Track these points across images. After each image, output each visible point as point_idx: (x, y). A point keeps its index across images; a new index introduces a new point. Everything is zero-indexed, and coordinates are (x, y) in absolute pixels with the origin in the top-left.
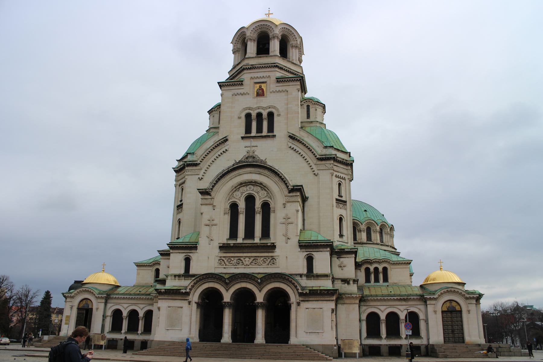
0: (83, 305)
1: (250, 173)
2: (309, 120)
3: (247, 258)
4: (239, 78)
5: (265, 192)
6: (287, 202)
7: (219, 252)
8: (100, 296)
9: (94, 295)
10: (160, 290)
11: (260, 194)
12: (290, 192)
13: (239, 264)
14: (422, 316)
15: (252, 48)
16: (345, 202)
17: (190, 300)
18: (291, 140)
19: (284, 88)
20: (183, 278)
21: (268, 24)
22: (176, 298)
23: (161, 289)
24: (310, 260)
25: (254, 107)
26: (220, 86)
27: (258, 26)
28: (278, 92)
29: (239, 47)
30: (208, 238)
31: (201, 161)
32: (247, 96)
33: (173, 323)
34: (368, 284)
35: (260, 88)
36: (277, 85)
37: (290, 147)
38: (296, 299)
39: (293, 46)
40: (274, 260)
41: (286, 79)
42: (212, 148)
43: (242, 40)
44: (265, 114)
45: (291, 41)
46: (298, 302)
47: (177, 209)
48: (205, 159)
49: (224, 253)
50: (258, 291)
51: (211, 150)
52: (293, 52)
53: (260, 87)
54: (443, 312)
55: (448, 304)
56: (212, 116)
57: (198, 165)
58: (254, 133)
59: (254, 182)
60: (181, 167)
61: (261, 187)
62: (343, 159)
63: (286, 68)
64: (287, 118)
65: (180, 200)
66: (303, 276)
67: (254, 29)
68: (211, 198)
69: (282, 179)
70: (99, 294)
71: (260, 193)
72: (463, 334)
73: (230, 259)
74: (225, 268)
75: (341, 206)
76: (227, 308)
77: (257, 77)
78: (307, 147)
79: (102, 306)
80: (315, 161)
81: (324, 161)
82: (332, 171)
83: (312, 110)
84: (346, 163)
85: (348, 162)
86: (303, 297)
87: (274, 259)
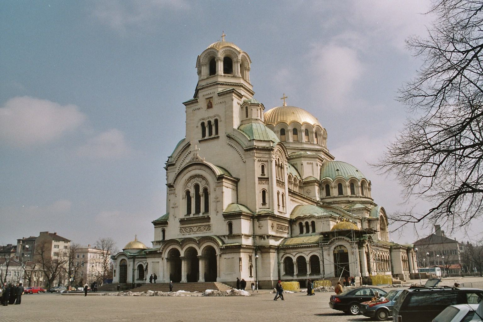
1: (195, 169)
3: (195, 227)
5: (205, 181)
11: (202, 183)
14: (320, 259)
15: (205, 70)
16: (268, 178)
17: (163, 257)
19: (223, 100)
24: (230, 225)
27: (207, 53)
31: (176, 162)
34: (301, 235)
37: (228, 144)
40: (210, 227)
44: (213, 122)
49: (183, 224)
50: (198, 249)
51: (181, 153)
52: (235, 67)
53: (210, 101)
54: (335, 254)
55: (339, 248)
58: (207, 137)
61: (202, 178)
62: (264, 147)
63: (226, 83)
67: (204, 56)
74: (183, 235)
75: (264, 182)
79: (132, 263)
82: (255, 158)
84: (268, 149)
85: (269, 148)
87: (210, 226)
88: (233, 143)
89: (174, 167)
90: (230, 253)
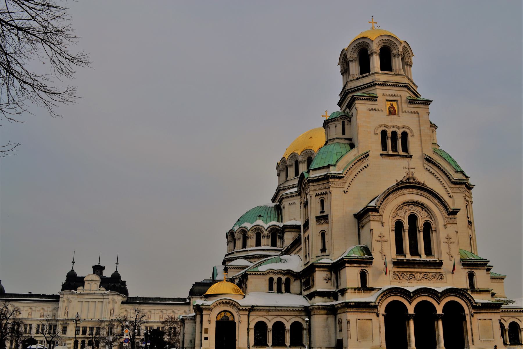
0: (221, 317)
3: (418, 273)
4: (367, 92)
5: (426, 213)
6: (447, 223)
7: (392, 267)
9: (237, 307)
10: (350, 304)
12: (448, 215)
13: (411, 278)
15: (375, 62)
17: (378, 313)
18: (427, 162)
19: (416, 110)
20: (363, 291)
22: (364, 311)
23: (351, 303)
24: (471, 276)
25: (389, 125)
28: (409, 113)
29: (355, 56)
30: (381, 253)
31: (345, 175)
32: (381, 112)
35: (392, 106)
36: (408, 106)
37: (426, 169)
38: (470, 311)
39: (408, 64)
40: (441, 275)
43: (360, 50)
45: (405, 58)
46: (473, 314)
47: (316, 220)
48: (348, 173)
49: (397, 268)
50: (438, 305)
51: (354, 164)
52: (407, 70)
53: (392, 105)
56: (334, 126)
57: (342, 178)
59: (415, 203)
60: (320, 177)
64: (421, 139)
65: (320, 211)
66: (469, 291)
68: (379, 215)
71: (421, 213)
73: (404, 274)
74: (399, 282)
76: (411, 320)
78: (443, 170)
79: (244, 319)
80: (450, 184)
81: (457, 185)
85: (470, 186)
86: (475, 309)
87: (442, 274)
88: (434, 169)
90: (486, 312)
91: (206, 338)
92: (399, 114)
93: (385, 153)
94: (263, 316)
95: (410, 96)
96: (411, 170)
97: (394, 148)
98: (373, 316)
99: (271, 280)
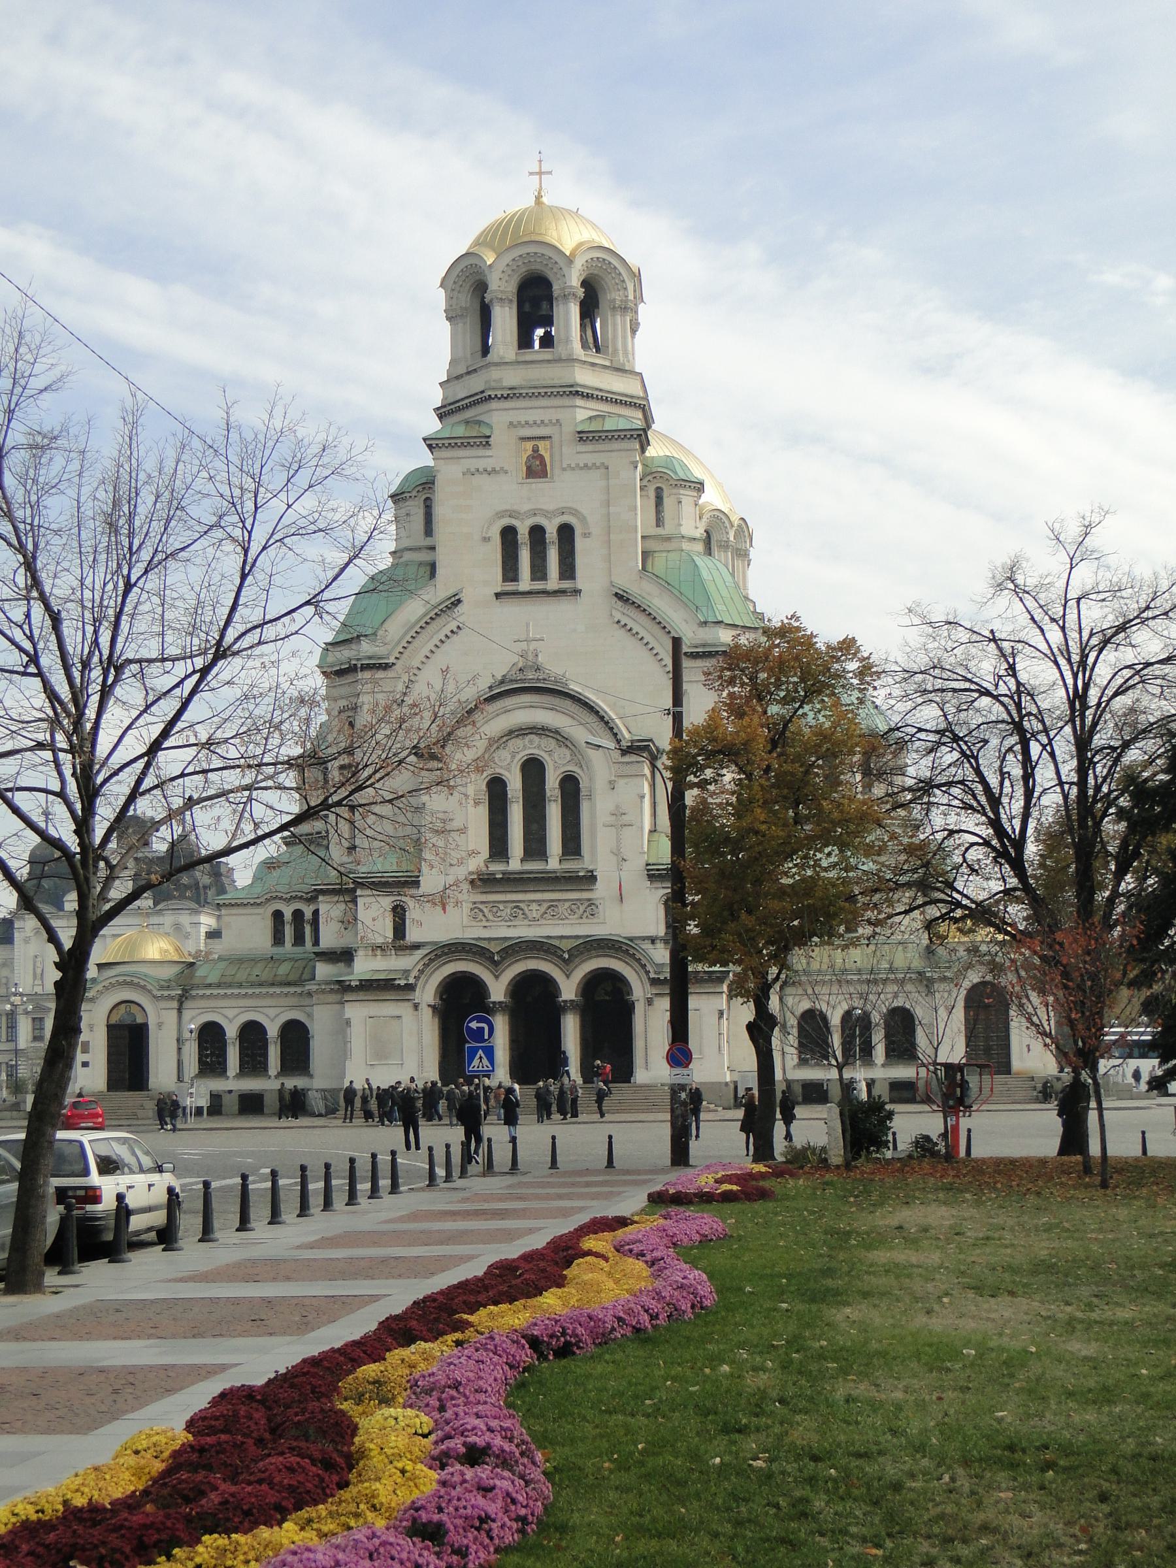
2: (660, 531)
5: (568, 752)
8: (166, 993)
9: (149, 991)
12: (623, 755)
15: (505, 321)
18: (620, 603)
19: (598, 459)
21: (548, 252)
26: (430, 447)
28: (581, 468)
33: (381, 1052)
37: (618, 622)
41: (603, 435)
42: (422, 623)
52: (615, 325)
53: (536, 450)
63: (600, 394)
64: (609, 541)
69: (607, 723)
70: (162, 988)
72: (1008, 1055)
77: (527, 423)
78: (660, 623)
83: (668, 502)
89: (390, 673)
91: (85, 1064)
92: (552, 477)
93: (510, 587)
94: (213, 1010)
95: (595, 413)
96: (533, 645)
97: (539, 571)
98: (404, 1010)
99: (278, 915)
